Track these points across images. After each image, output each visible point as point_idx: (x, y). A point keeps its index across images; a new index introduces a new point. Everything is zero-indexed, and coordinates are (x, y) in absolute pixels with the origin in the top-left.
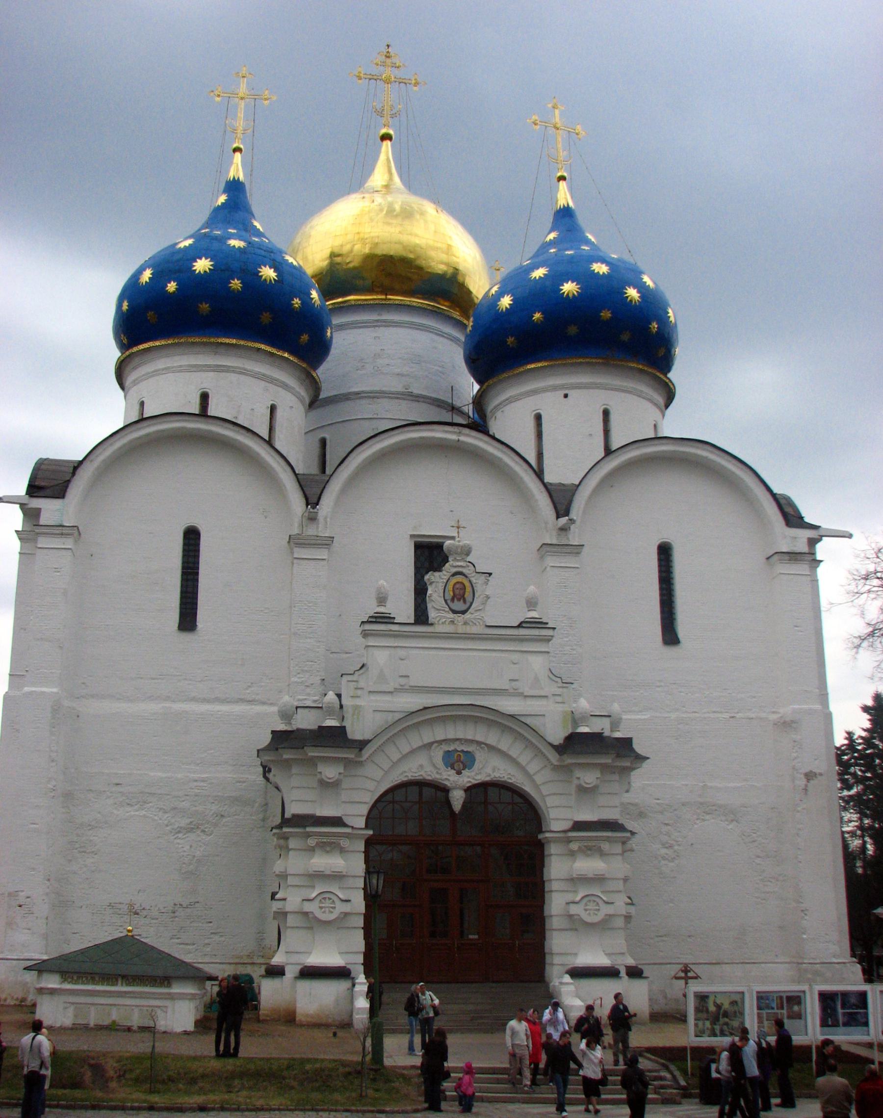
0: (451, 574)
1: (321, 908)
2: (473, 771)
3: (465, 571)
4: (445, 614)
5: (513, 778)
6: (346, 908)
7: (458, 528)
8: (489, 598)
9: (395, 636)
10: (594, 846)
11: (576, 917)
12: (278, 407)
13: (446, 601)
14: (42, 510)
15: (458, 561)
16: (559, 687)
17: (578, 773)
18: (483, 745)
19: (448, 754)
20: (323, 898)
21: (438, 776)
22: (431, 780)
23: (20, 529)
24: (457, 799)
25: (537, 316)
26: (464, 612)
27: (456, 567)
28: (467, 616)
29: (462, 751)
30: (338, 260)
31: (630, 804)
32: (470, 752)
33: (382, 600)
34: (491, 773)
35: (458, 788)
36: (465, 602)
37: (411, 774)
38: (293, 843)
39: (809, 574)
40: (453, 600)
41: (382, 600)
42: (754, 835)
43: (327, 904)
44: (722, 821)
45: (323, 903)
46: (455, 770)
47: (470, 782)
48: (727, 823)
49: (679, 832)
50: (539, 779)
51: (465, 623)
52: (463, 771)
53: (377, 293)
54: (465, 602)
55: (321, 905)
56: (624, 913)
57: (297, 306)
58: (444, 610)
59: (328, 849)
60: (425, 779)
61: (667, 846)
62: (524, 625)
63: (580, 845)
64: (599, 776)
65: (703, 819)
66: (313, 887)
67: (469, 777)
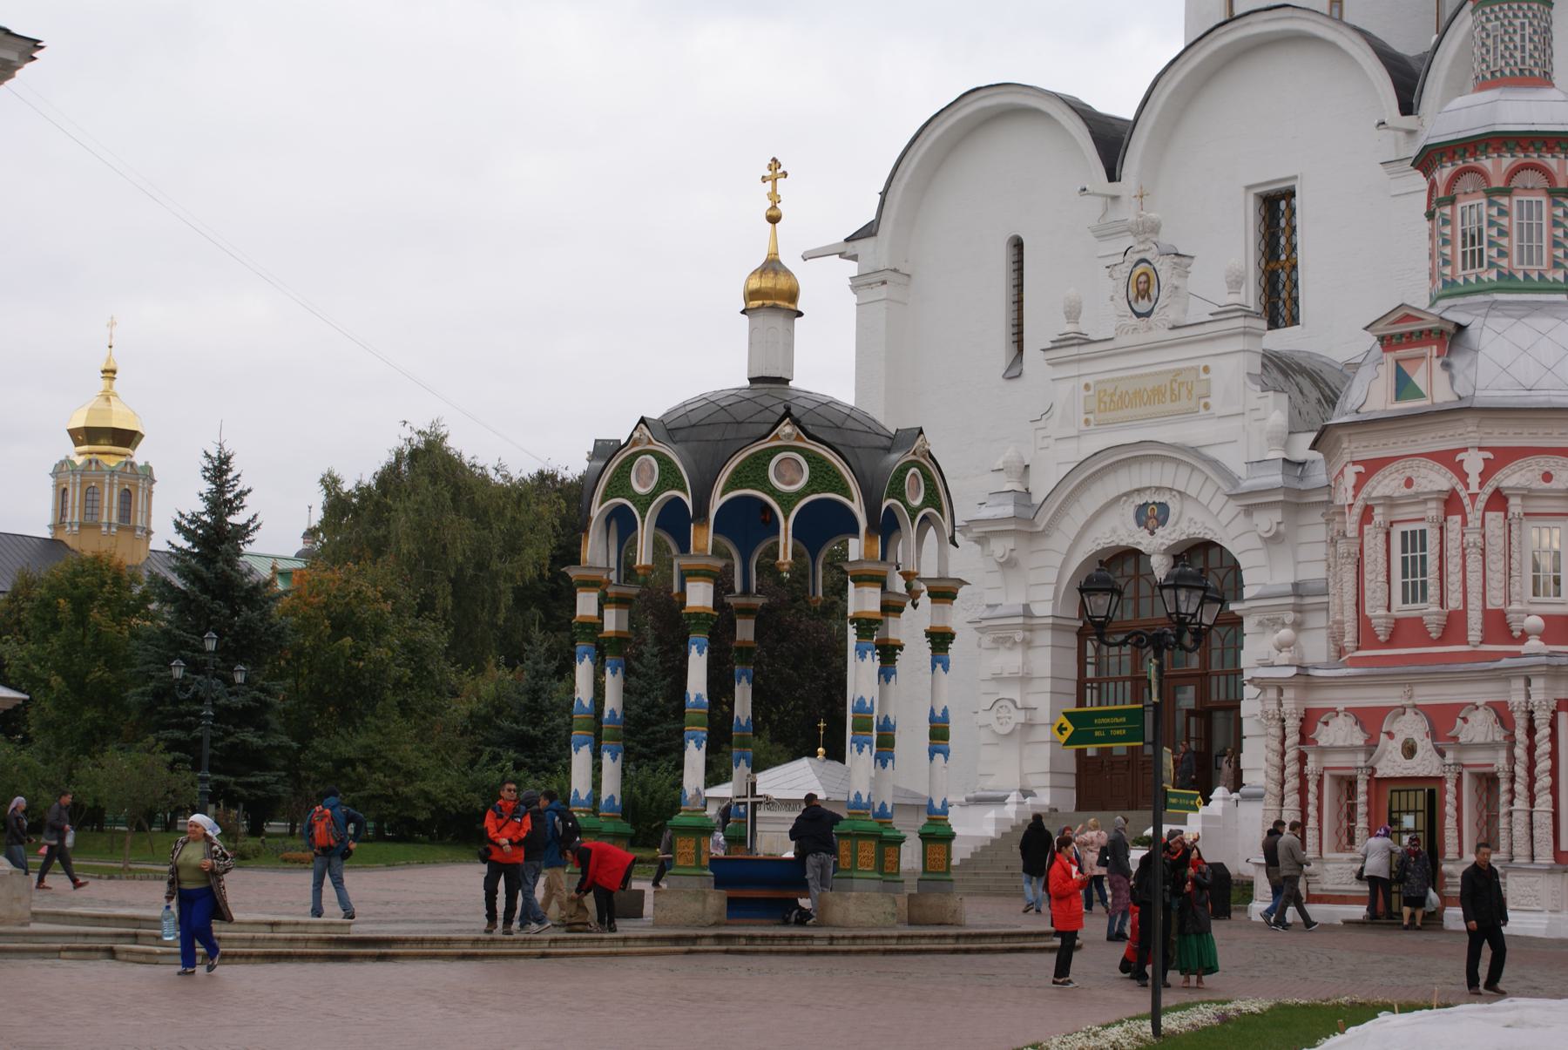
1: (998, 718)
3: (1148, 256)
6: (1020, 717)
7: (1141, 197)
13: (1129, 303)
15: (1143, 242)
18: (1174, 493)
19: (1141, 510)
24: (1160, 567)
26: (1148, 314)
27: (1139, 252)
28: (1153, 316)
29: (1154, 503)
33: (1073, 314)
36: (1150, 300)
37: (1104, 540)
41: (1073, 314)
43: (1003, 713)
54: (1150, 300)
59: (1008, 645)
63: (1261, 618)
67: (1162, 537)
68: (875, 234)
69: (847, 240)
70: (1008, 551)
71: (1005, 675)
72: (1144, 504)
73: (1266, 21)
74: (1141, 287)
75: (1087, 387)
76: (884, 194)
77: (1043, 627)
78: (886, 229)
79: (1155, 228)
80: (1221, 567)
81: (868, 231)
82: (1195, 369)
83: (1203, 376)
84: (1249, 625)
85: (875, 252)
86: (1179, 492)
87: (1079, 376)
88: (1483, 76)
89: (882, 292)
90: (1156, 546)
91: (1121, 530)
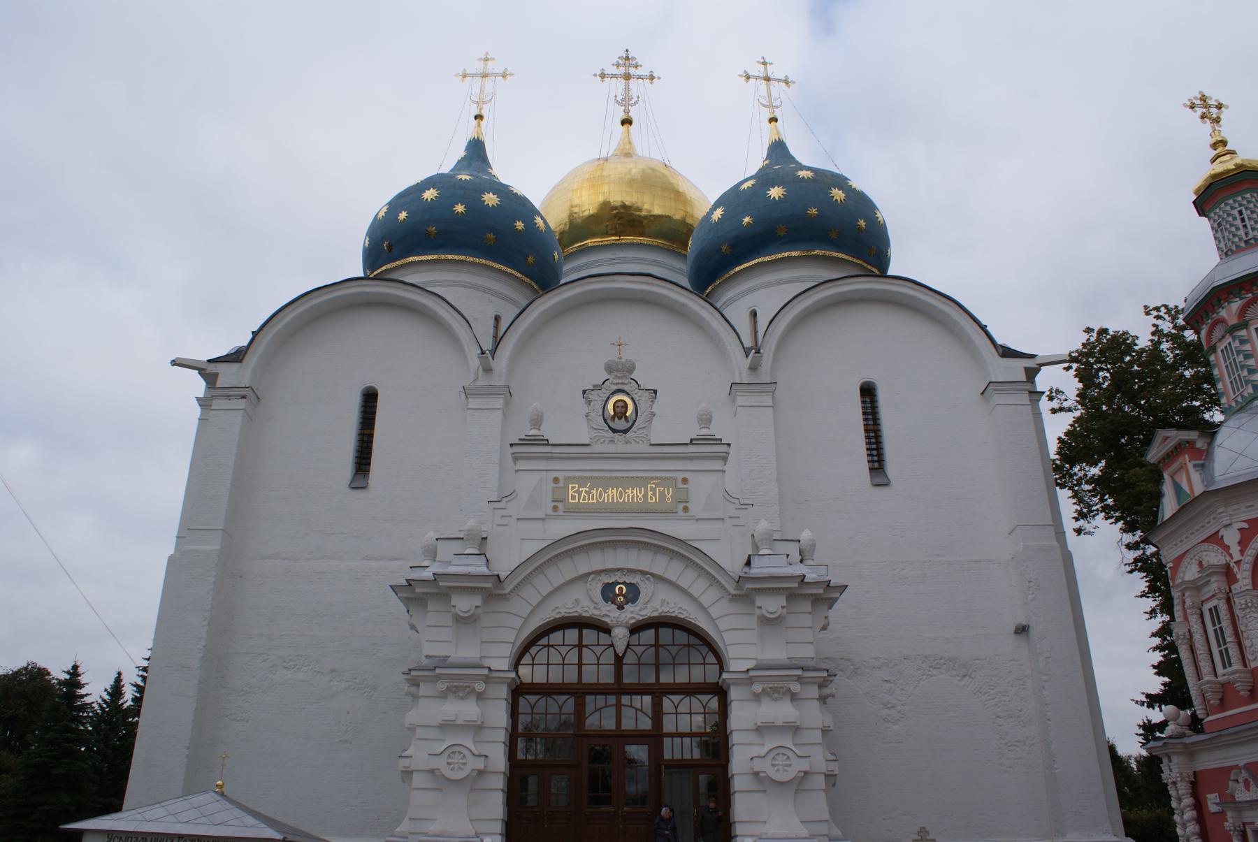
0: (611, 392)
2: (637, 605)
3: (626, 388)
4: (604, 434)
5: (685, 613)
6: (479, 764)
8: (654, 415)
9: (548, 459)
10: (782, 688)
11: (762, 775)
12: (502, 318)
14: (220, 376)
15: (619, 378)
16: (737, 509)
17: (760, 601)
18: (648, 576)
20: (452, 753)
21: (597, 612)
22: (588, 617)
23: (202, 396)
25: (747, 220)
26: (625, 431)
28: (629, 434)
29: (624, 583)
30: (576, 210)
31: (842, 659)
32: (633, 584)
34: (658, 607)
35: (619, 626)
38: (424, 689)
39: (1029, 403)
40: (613, 418)
41: (537, 422)
42: (992, 692)
44: (952, 676)
45: (453, 758)
46: (615, 604)
47: (634, 618)
48: (958, 678)
49: (902, 689)
50: (714, 612)
51: (627, 442)
52: (625, 606)
53: (612, 235)
55: (450, 761)
56: (824, 770)
57: (520, 228)
58: (603, 430)
59: (461, 694)
60: (580, 616)
61: (889, 706)
62: (694, 442)
64: (785, 604)
65: (929, 675)
66: (444, 740)
68: (240, 361)
69: (210, 361)
70: (474, 607)
71: (460, 721)
72: (613, 583)
73: (628, 282)
74: (618, 410)
75: (556, 480)
76: (255, 334)
77: (500, 681)
78: (251, 360)
79: (631, 369)
80: (673, 645)
81: (237, 356)
82: (675, 479)
83: (681, 486)
84: (734, 694)
85: (228, 375)
86: (652, 575)
87: (547, 470)
88: (1237, 246)
89: (242, 403)
90: (620, 618)
91: (586, 602)
